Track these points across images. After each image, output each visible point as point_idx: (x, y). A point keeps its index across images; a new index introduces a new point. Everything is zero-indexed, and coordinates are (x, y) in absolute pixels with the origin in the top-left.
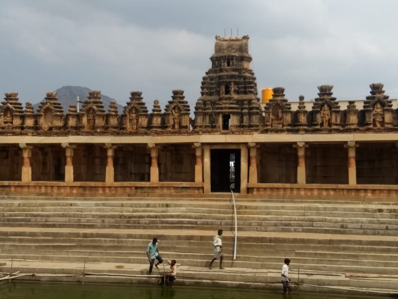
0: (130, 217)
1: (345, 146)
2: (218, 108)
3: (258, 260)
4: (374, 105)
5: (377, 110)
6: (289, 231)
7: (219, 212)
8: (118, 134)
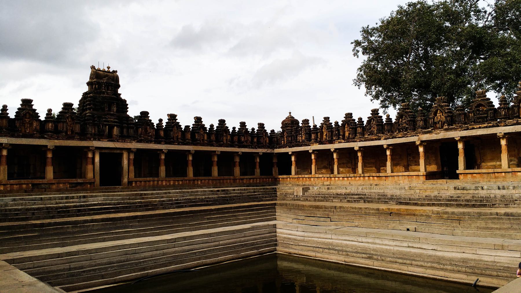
0: (57, 208)
1: (187, 153)
2: (105, 121)
3: (190, 225)
4: (199, 129)
5: (202, 133)
6: (182, 207)
7: (129, 199)
8: (13, 136)
